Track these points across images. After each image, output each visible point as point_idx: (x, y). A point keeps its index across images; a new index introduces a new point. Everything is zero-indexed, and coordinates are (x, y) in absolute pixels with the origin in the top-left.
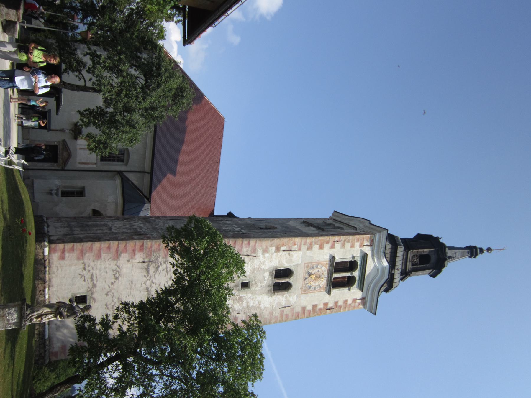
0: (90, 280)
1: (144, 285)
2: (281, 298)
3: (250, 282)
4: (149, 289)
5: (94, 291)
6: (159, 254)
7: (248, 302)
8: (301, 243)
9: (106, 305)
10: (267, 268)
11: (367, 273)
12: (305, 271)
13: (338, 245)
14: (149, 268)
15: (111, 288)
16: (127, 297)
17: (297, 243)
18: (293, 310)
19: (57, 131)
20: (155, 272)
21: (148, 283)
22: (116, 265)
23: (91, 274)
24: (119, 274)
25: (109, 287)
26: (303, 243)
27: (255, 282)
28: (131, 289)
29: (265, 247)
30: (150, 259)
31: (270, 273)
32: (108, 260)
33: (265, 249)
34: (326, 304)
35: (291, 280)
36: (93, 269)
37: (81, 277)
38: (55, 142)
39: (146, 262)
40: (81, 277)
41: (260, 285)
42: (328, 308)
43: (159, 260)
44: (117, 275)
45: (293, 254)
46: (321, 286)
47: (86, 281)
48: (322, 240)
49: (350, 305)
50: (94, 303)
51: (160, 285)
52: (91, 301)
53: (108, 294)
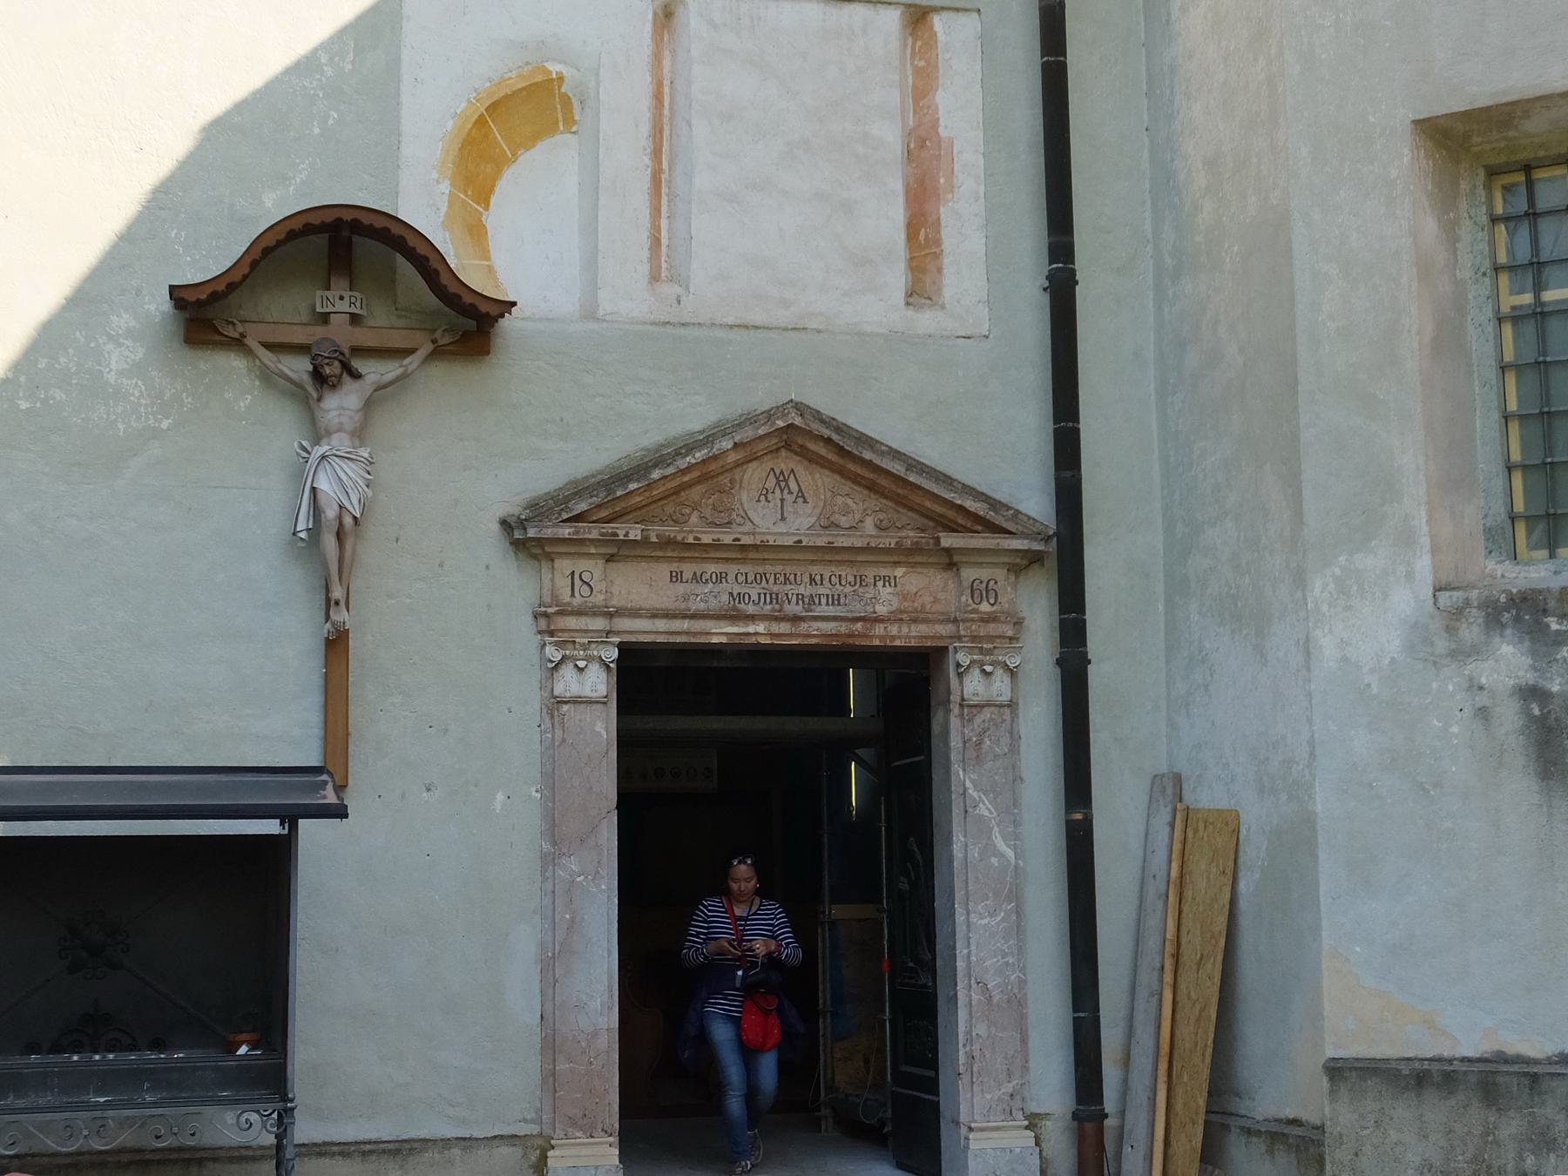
19: (336, 645)
38: (568, 683)
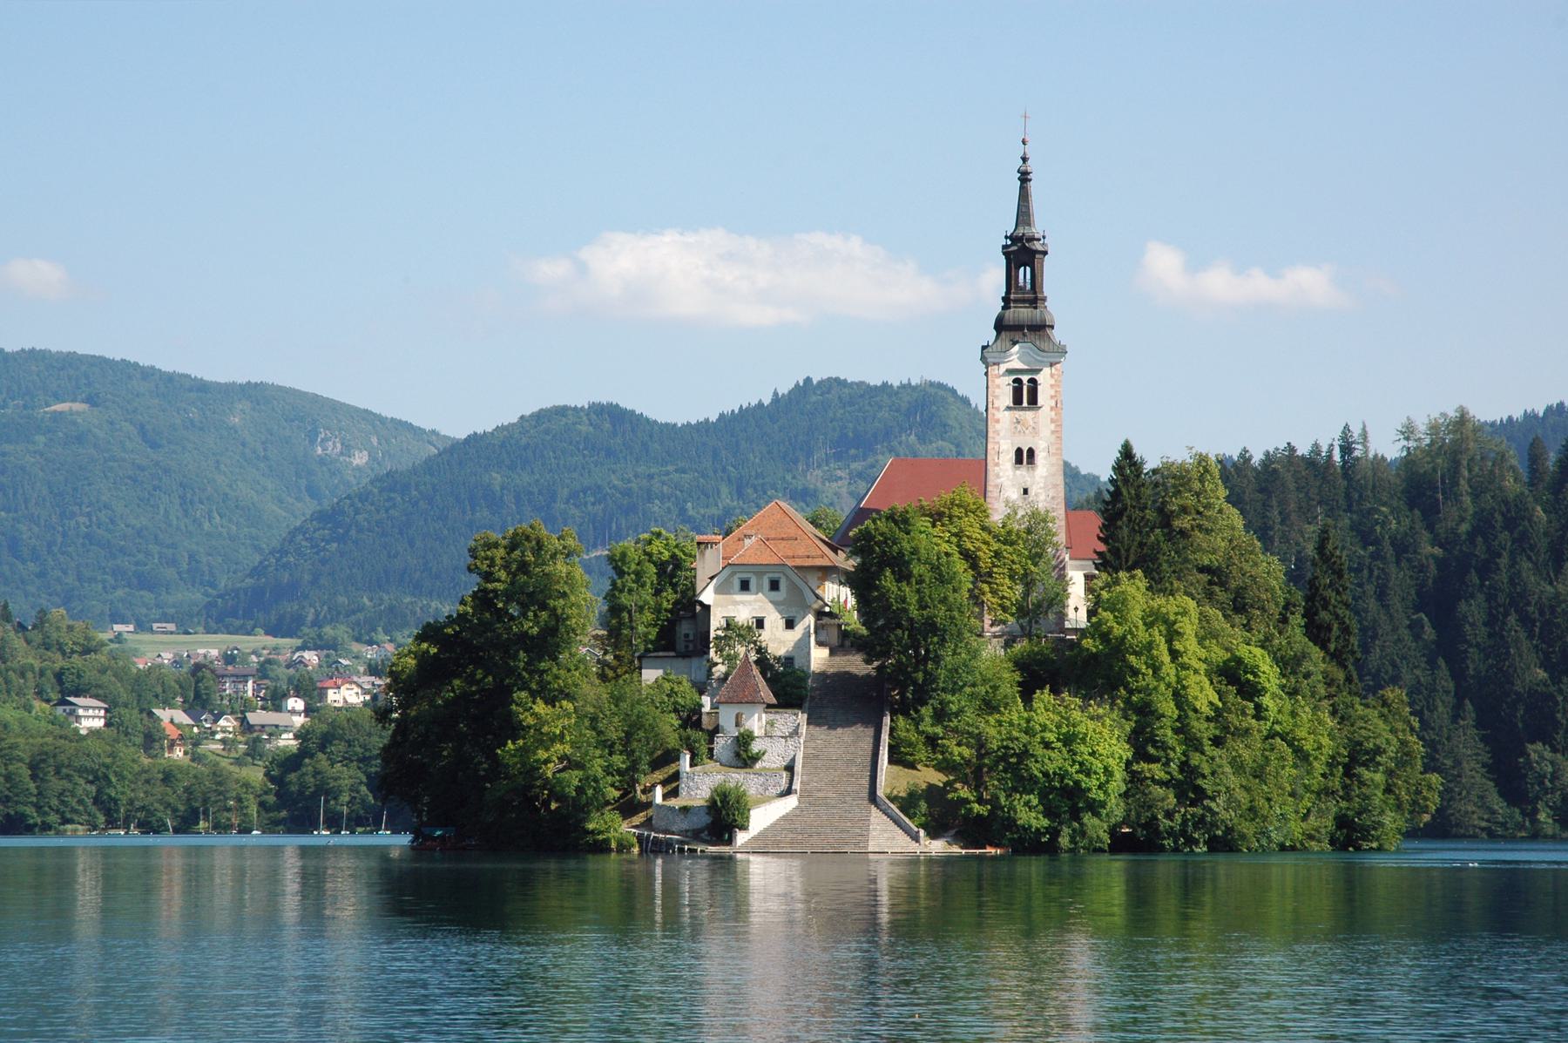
2: (1040, 457)
11: (1026, 367)
13: (995, 405)
34: (1052, 409)
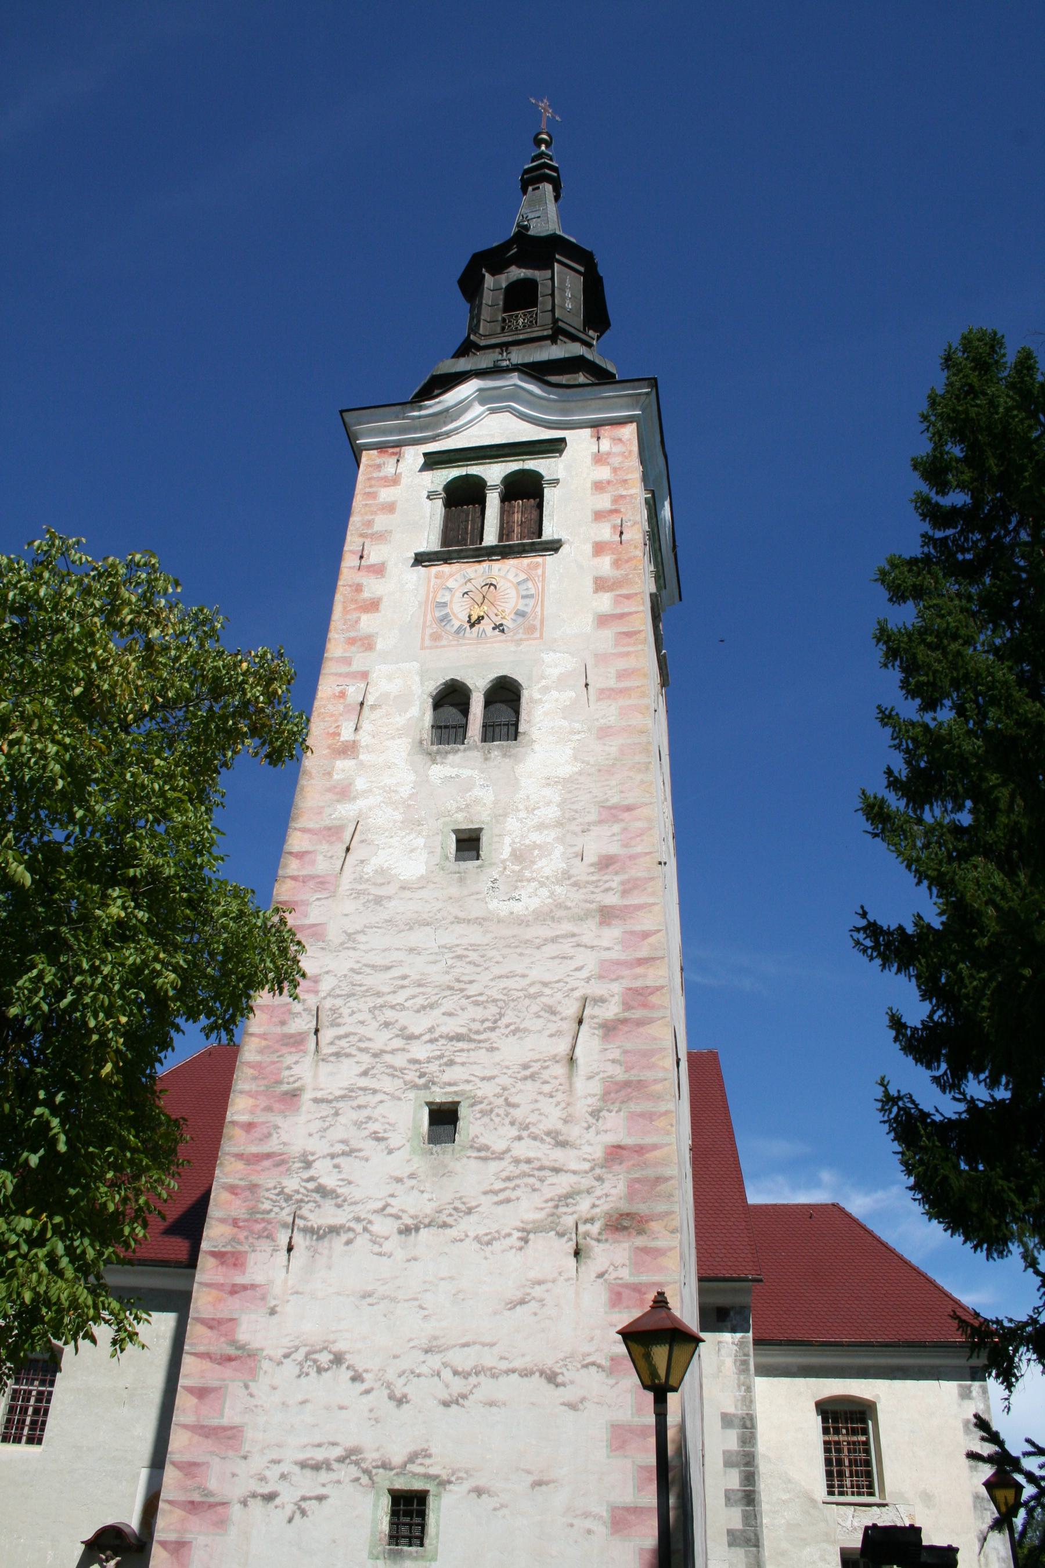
0: (324, 1476)
1: (387, 1247)
3: (455, 832)
4: (409, 1221)
5: (376, 1455)
6: (268, 1190)
7: (541, 827)
8: (340, 675)
9: (446, 1404)
10: (412, 777)
12: (455, 643)
13: (373, 557)
14: (319, 1228)
15: (377, 1385)
16: (426, 1313)
17: (338, 689)
18: (601, 658)
20: (339, 1200)
21: (382, 1226)
22: (280, 1363)
23: (296, 1469)
24: (321, 1351)
25: (367, 1392)
26: (344, 669)
27: (459, 810)
28: (394, 1300)
29: (329, 796)
30: (285, 1225)
31: (434, 761)
32: (251, 1395)
33: (337, 794)
34: (599, 548)
35: (478, 685)
36: (279, 1462)
37: (303, 1513)
39: (291, 1238)
40: (303, 1513)
41: (477, 792)
42: (617, 538)
43: (297, 1187)
44: (324, 1358)
45: (377, 694)
46: (523, 576)
47: (322, 1491)
48: (345, 608)
49: (615, 470)
50: (429, 1456)
51: (399, 1180)
52: (420, 1470)
53: (398, 1395)
